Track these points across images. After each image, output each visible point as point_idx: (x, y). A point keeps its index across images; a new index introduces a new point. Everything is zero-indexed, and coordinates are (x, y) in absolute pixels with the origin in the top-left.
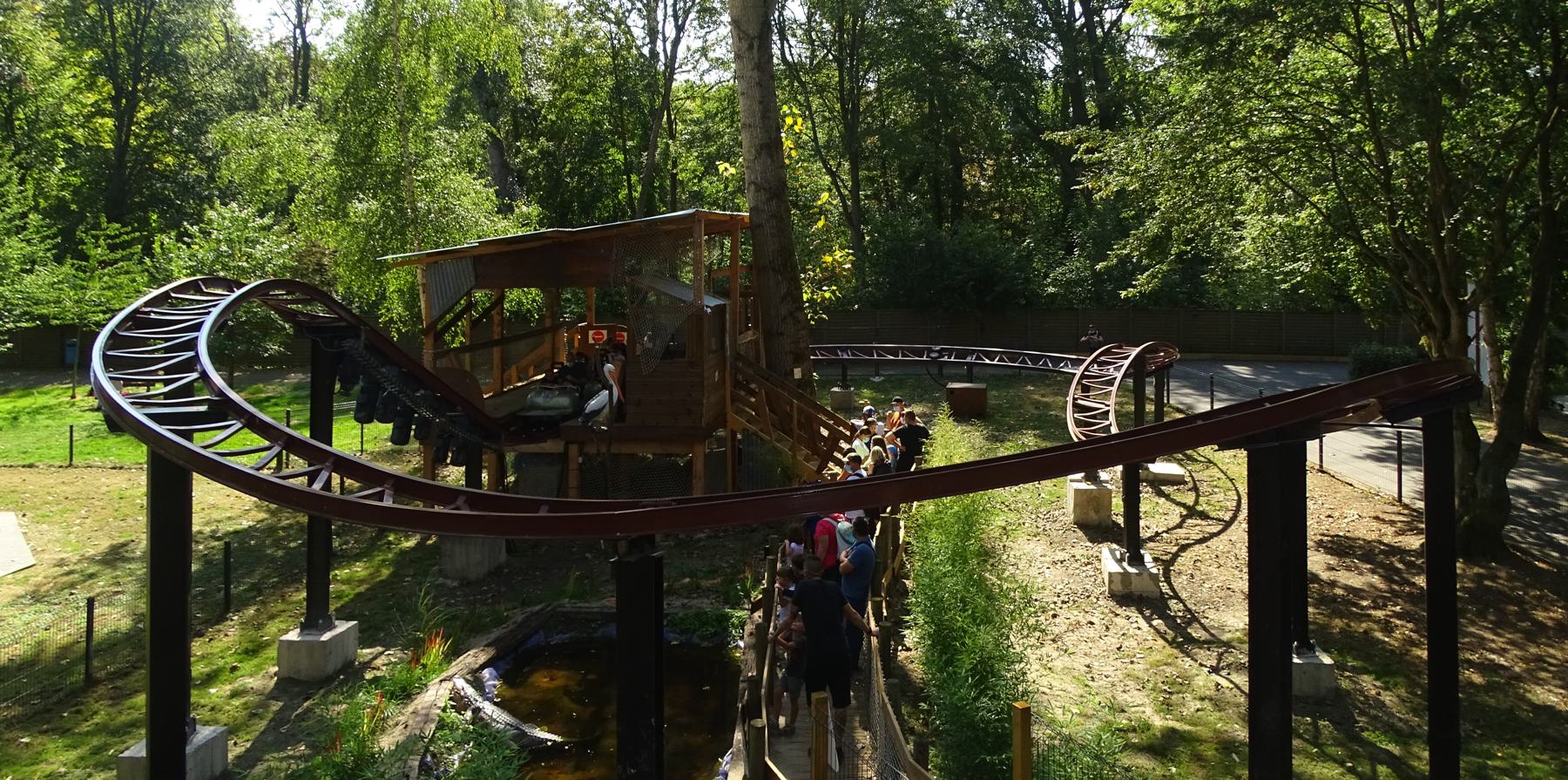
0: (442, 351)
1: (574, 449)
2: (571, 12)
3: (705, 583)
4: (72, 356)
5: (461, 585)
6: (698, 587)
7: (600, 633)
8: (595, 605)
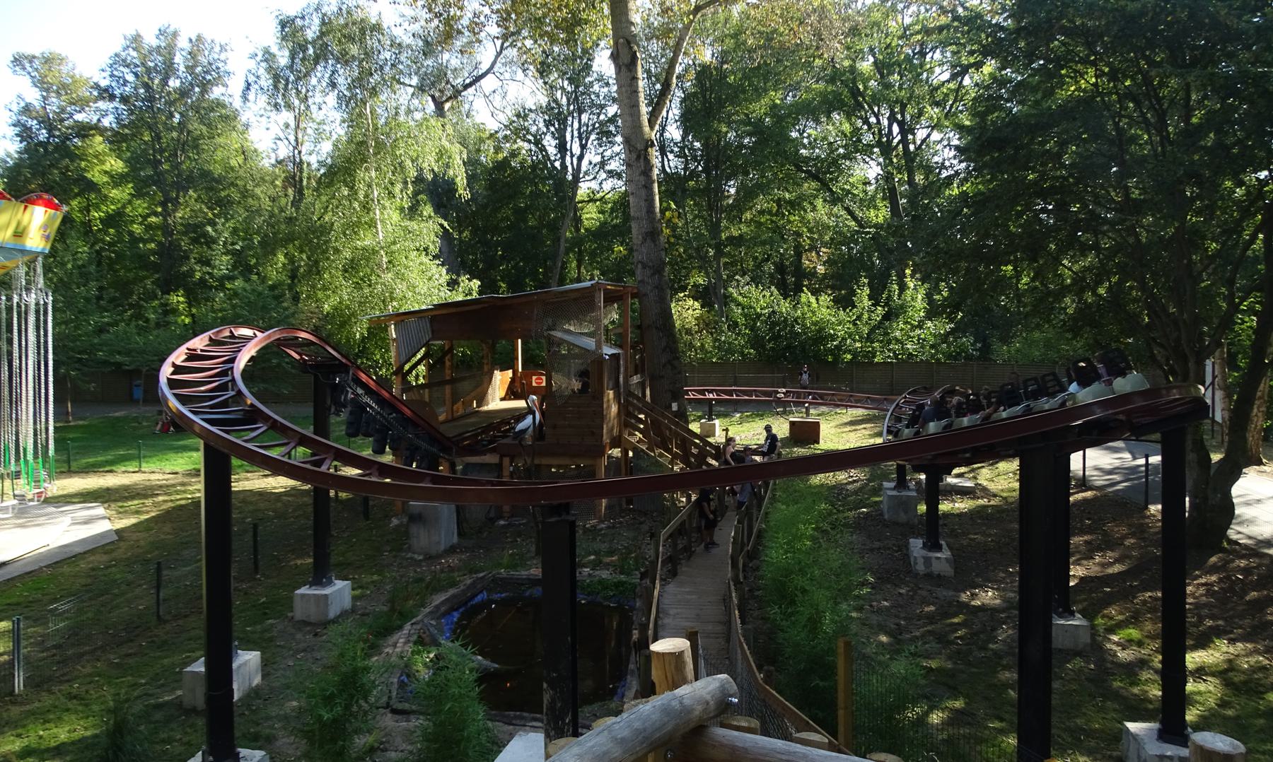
0: (407, 387)
1: (506, 461)
2: (500, 135)
3: (608, 560)
4: (138, 393)
5: (425, 559)
6: (601, 562)
7: (527, 594)
8: (524, 573)
